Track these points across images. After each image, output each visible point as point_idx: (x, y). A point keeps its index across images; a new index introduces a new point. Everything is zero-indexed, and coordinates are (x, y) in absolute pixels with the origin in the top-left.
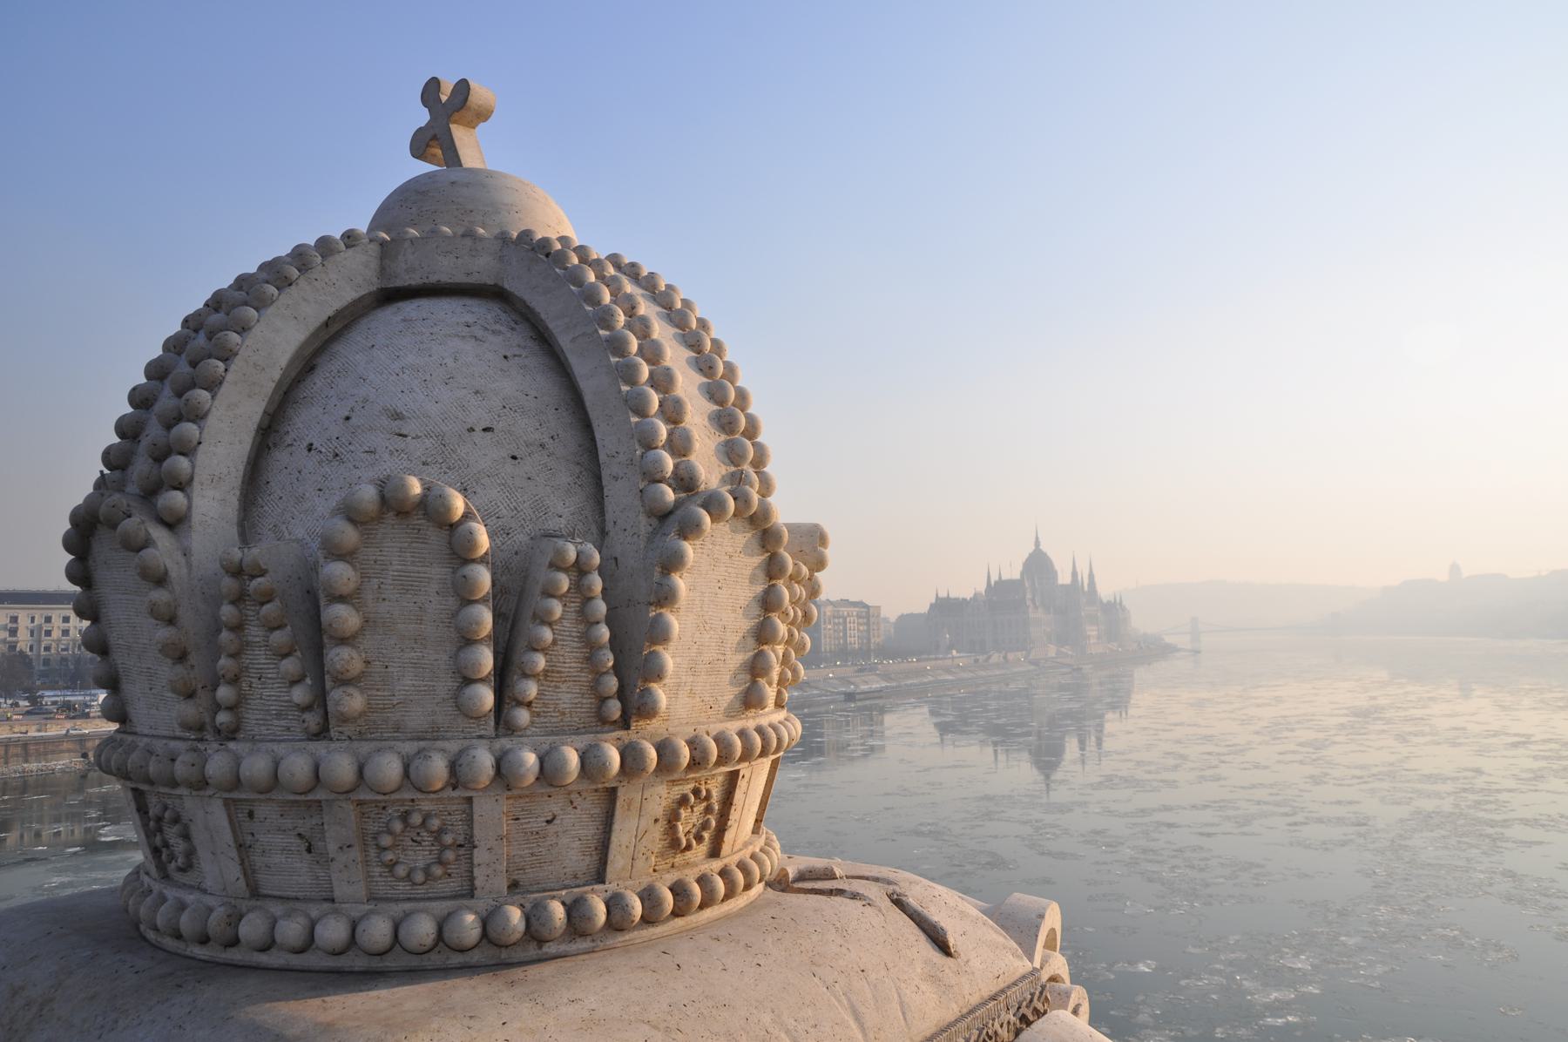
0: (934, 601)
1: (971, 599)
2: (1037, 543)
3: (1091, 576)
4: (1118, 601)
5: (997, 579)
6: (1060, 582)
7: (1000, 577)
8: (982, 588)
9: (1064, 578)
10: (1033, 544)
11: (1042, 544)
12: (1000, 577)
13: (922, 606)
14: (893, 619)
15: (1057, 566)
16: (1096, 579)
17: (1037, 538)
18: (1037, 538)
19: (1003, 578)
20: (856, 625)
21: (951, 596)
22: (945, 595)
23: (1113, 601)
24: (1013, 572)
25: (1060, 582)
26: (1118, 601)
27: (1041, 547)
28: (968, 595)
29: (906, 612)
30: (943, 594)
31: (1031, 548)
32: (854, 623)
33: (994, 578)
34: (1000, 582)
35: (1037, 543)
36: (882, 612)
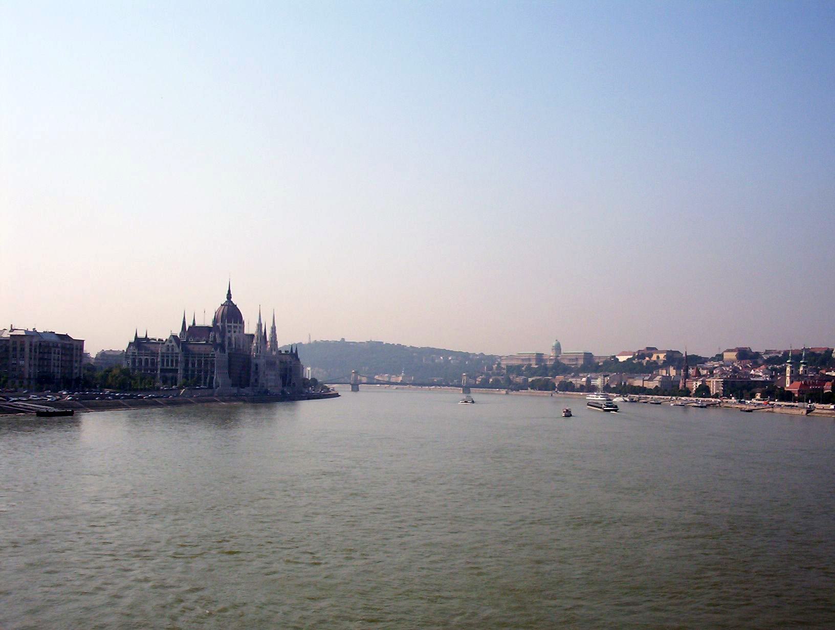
0: (133, 340)
1: (166, 340)
2: (229, 296)
3: (274, 329)
4: (294, 352)
5: (191, 324)
6: (246, 332)
7: (194, 324)
8: (177, 331)
9: (250, 328)
10: (226, 296)
11: (232, 297)
12: (194, 324)
13: (120, 343)
14: (93, 355)
15: (245, 318)
16: (277, 332)
17: (229, 291)
18: (229, 291)
19: (197, 324)
20: (60, 356)
21: (148, 337)
22: (144, 336)
23: (290, 351)
24: (206, 320)
25: (246, 332)
26: (294, 352)
27: (232, 300)
28: (165, 336)
29: (106, 348)
30: (141, 335)
31: (224, 299)
32: (59, 354)
33: (189, 323)
34: (194, 328)
35: (229, 296)
36: (84, 349)
